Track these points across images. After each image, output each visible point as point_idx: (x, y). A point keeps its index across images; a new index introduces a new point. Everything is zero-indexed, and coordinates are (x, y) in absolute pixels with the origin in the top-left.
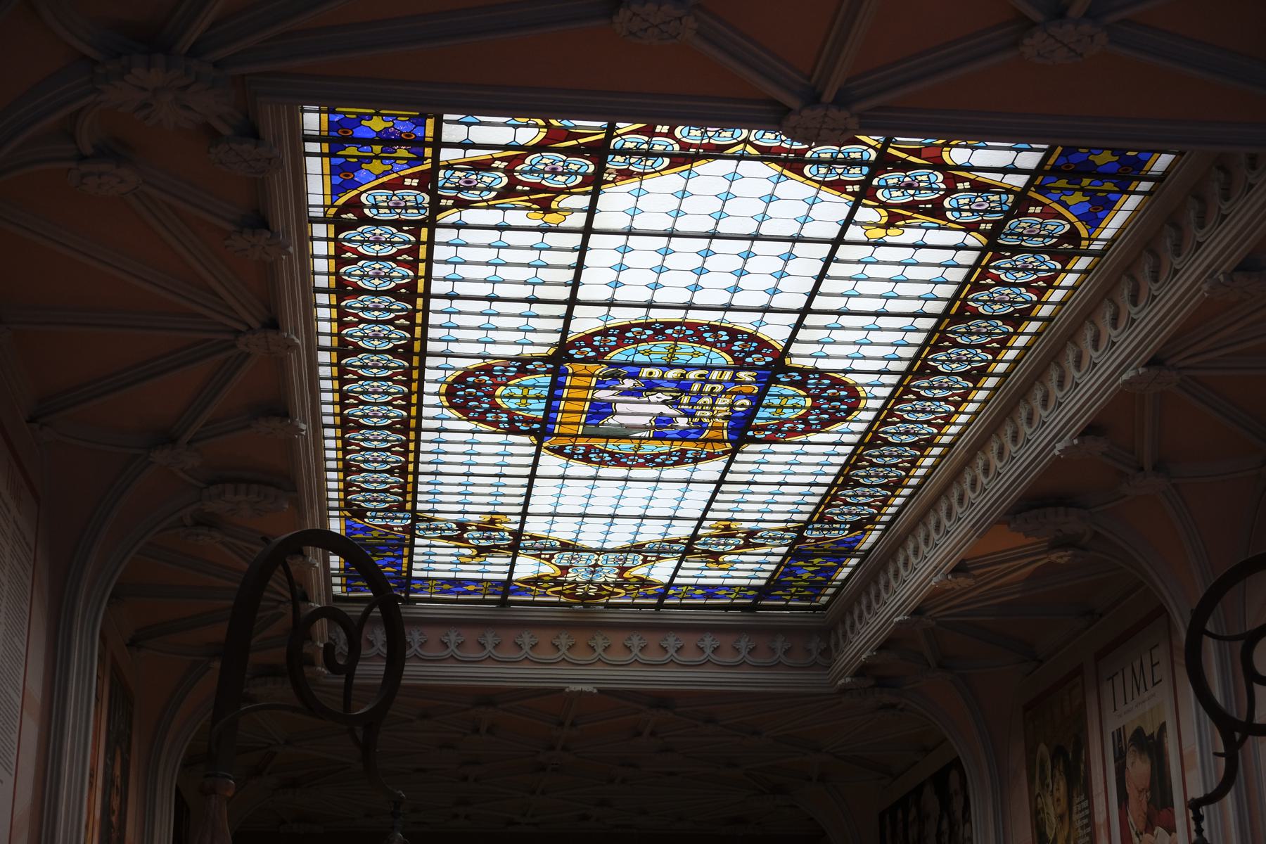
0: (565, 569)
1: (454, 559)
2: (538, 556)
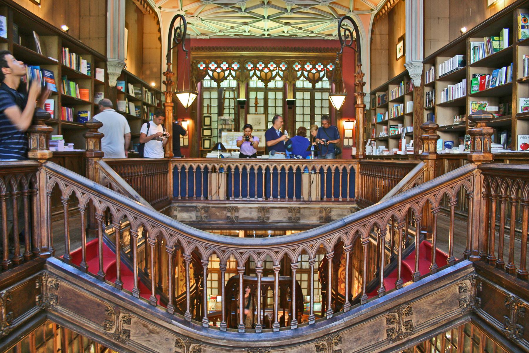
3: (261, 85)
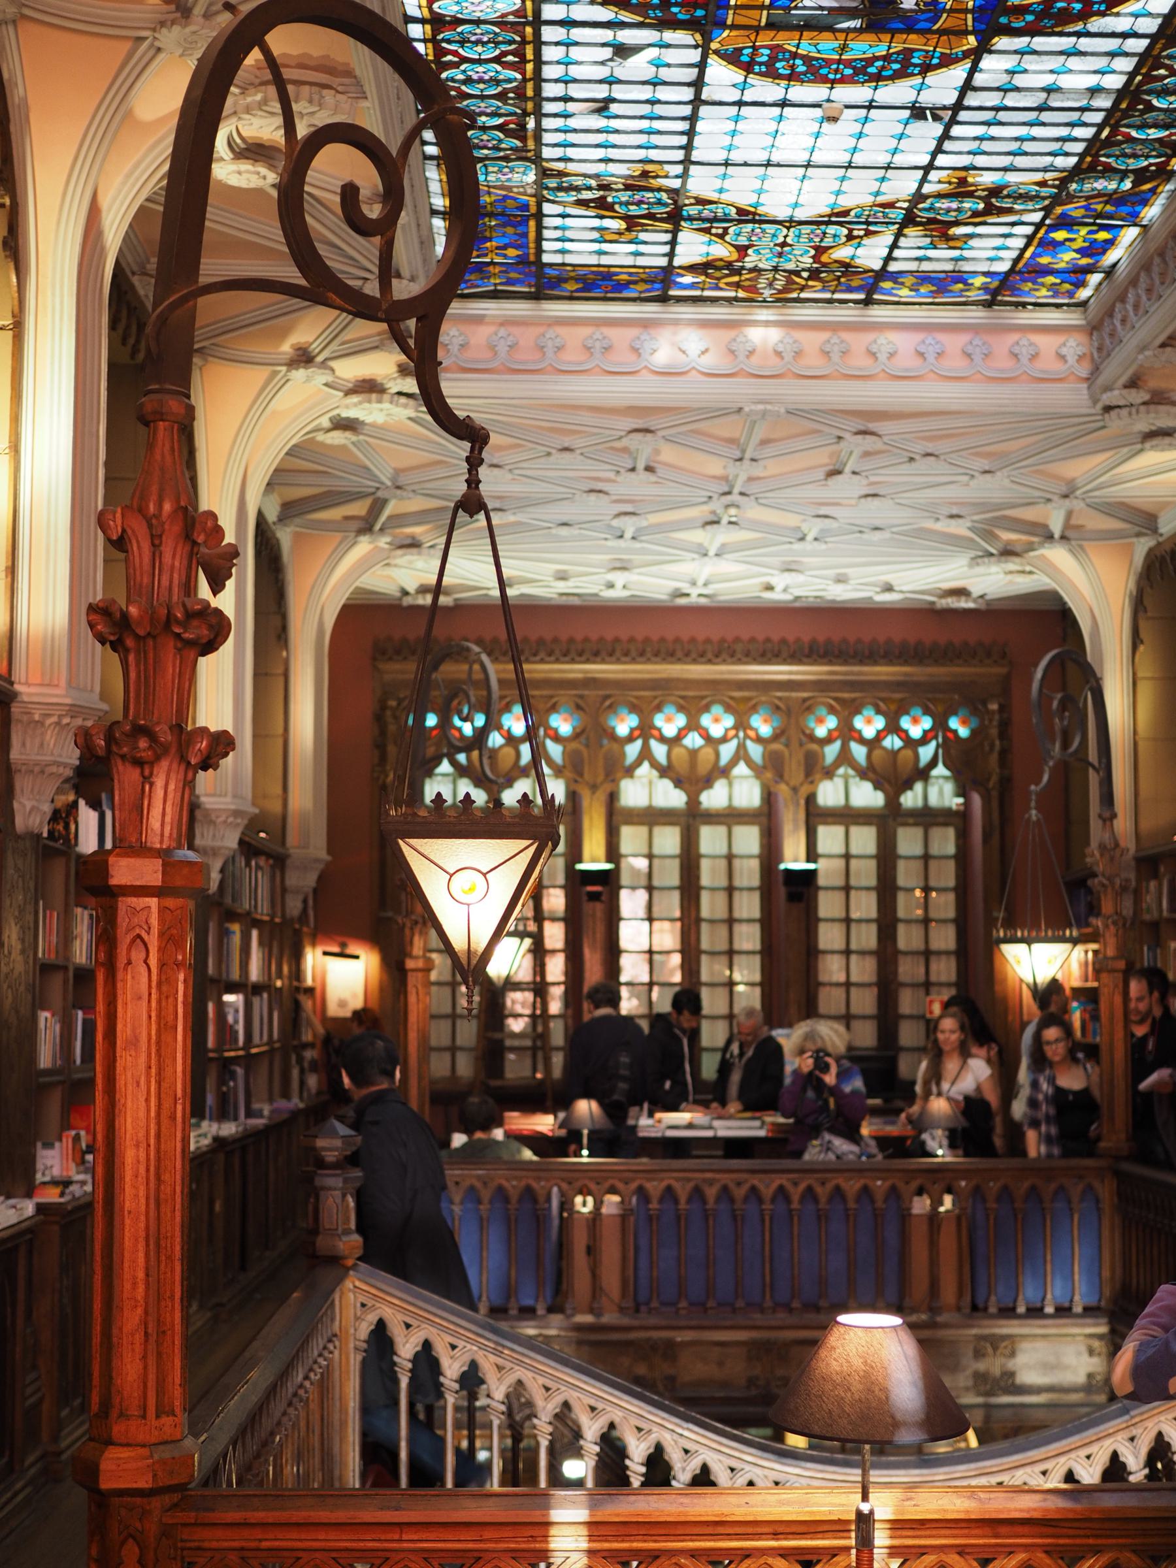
0: (742, 250)
1: (595, 235)
2: (707, 231)
3: (671, 797)
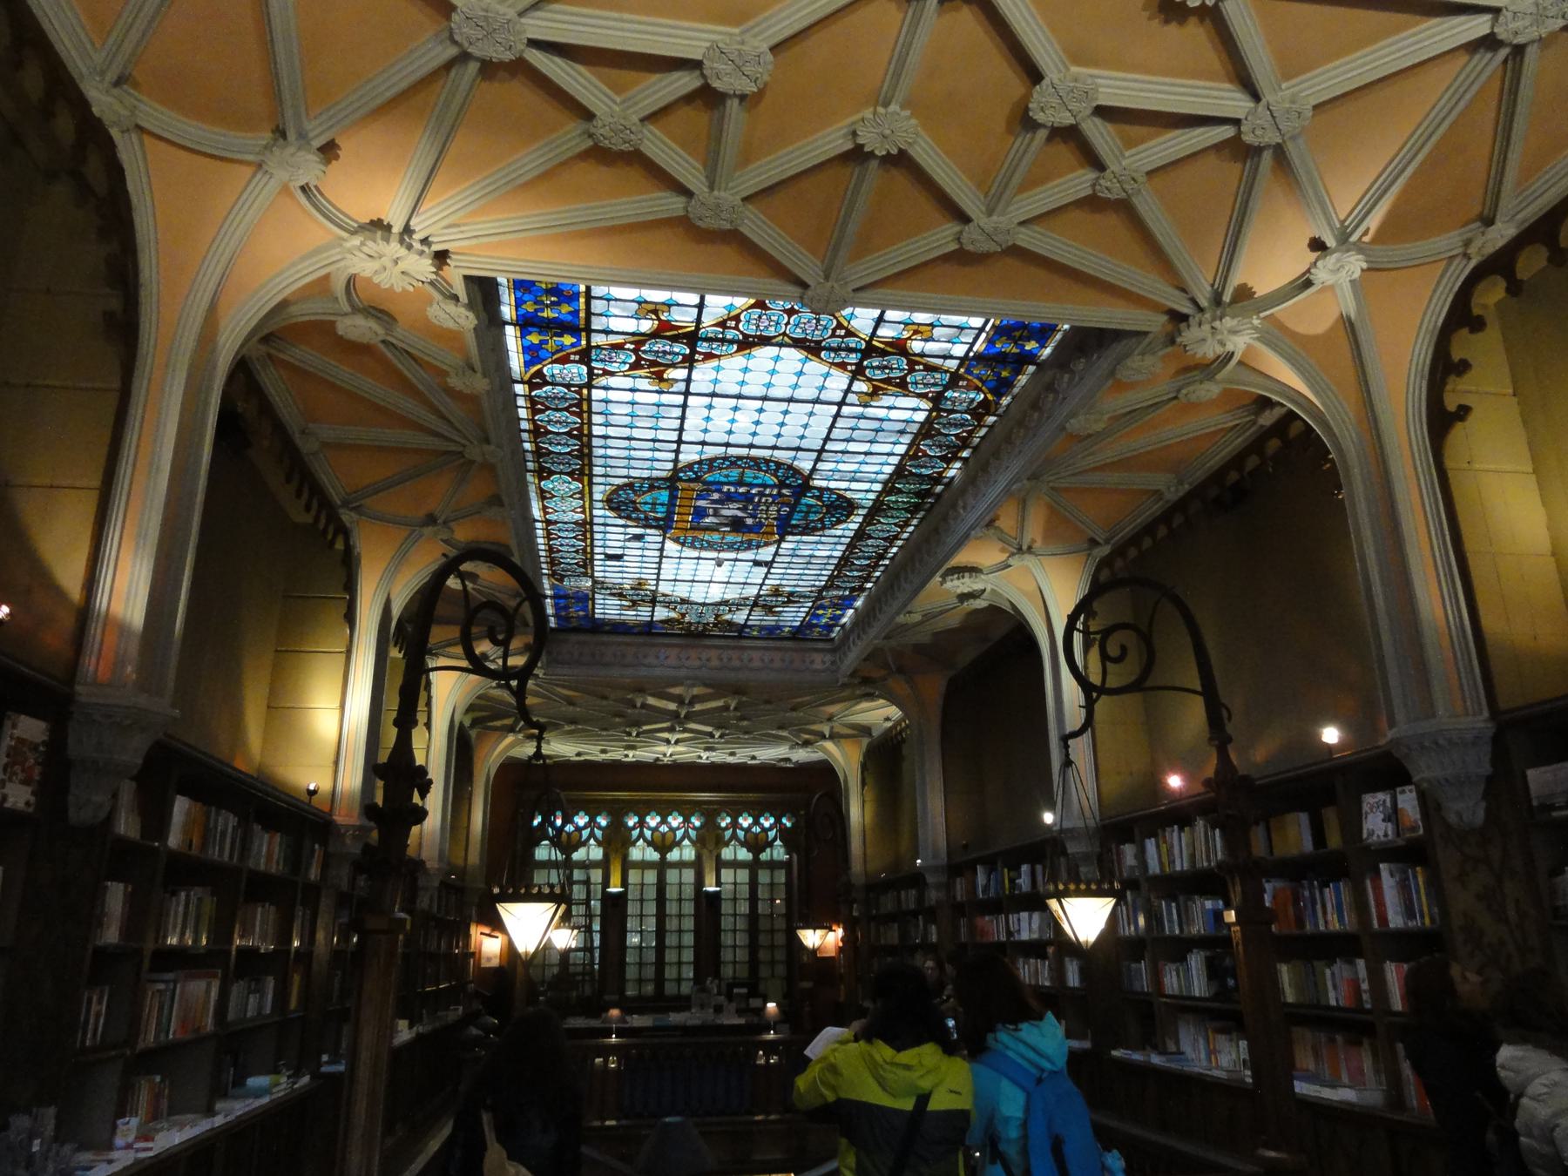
0: (683, 615)
2: (668, 607)
3: (652, 855)
